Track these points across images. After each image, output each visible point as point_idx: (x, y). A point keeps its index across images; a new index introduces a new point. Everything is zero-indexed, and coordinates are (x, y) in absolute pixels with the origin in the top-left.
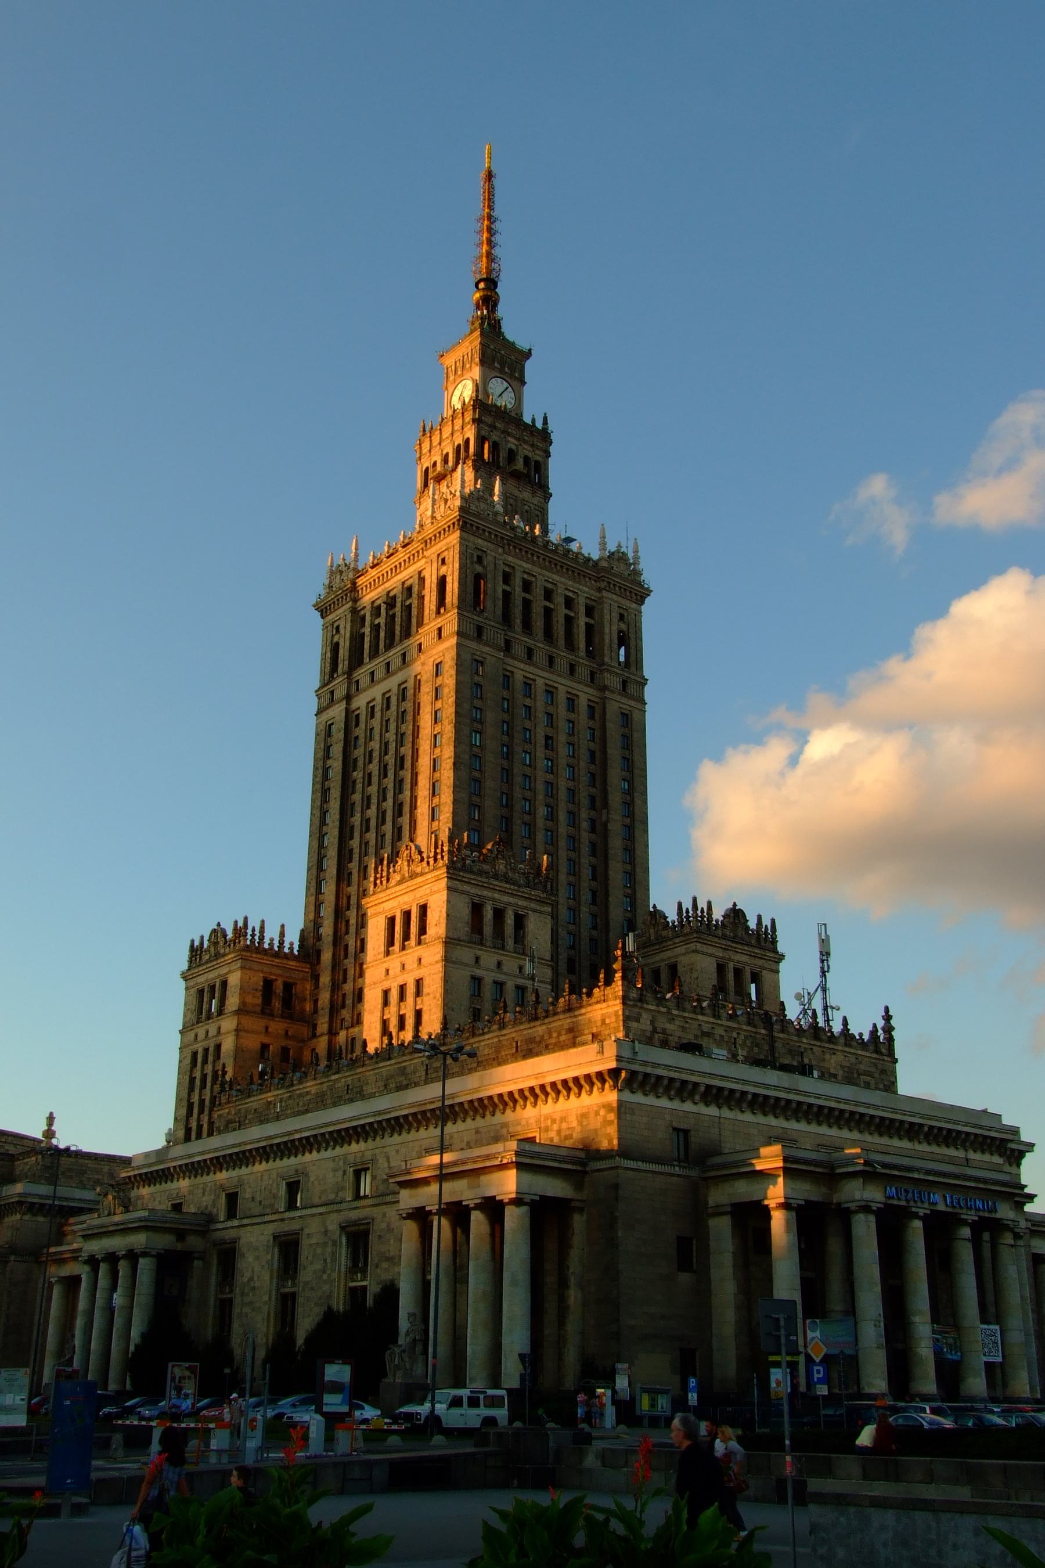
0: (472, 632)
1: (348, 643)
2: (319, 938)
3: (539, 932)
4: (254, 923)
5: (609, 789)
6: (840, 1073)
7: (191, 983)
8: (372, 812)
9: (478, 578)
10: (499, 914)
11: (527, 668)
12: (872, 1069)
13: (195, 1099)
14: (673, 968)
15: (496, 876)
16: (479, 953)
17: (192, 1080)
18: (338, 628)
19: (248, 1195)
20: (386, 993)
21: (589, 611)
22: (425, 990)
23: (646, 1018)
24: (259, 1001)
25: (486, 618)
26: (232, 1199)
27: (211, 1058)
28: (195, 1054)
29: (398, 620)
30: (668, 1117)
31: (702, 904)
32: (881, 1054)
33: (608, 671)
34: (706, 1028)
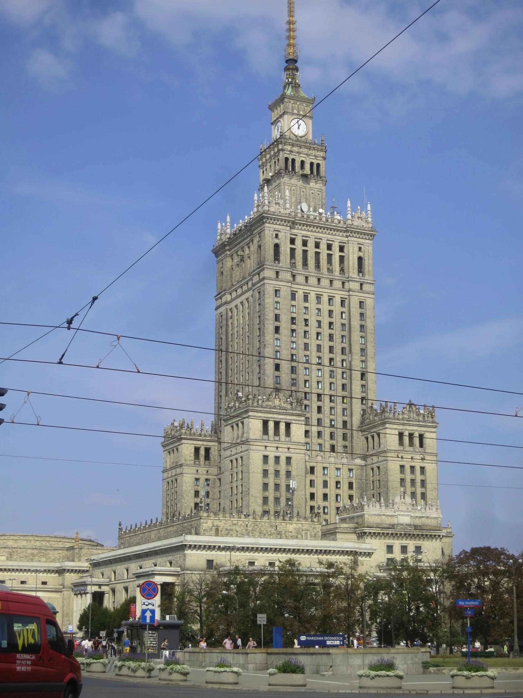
0: (274, 276)
3: (298, 431)
5: (352, 343)
6: (294, 531)
9: (277, 247)
11: (305, 288)
12: (309, 528)
15: (274, 407)
21: (341, 249)
22: (244, 463)
24: (193, 458)
25: (281, 267)
30: (205, 557)
32: (314, 522)
33: (351, 280)
34: (234, 522)
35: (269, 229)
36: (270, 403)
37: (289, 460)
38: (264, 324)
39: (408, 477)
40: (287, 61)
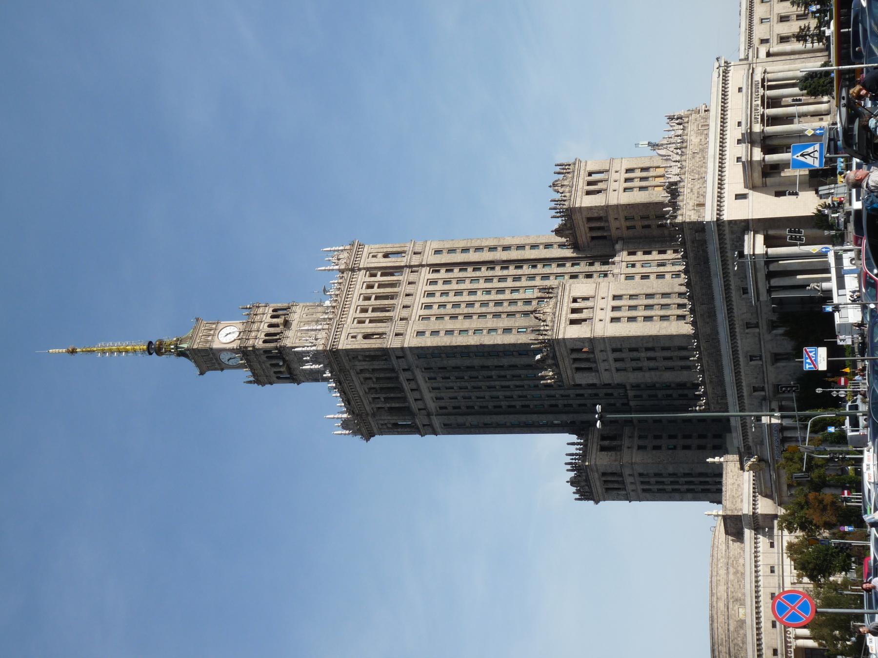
1: (395, 418)
2: (573, 423)
4: (568, 459)
6: (699, 138)
7: (601, 497)
8: (501, 394)
9: (366, 337)
10: (574, 311)
13: (670, 487)
14: (589, 220)
15: (554, 314)
16: (597, 320)
17: (659, 491)
18: (382, 425)
19: (754, 381)
20: (618, 370)
22: (619, 347)
23: (688, 213)
26: (755, 389)
27: (647, 480)
28: (644, 490)
29: (386, 385)
31: (553, 205)
34: (689, 191)
35: (344, 344)
36: (549, 319)
37: (615, 297)
38: (456, 347)
39: (637, 183)
40: (150, 354)
